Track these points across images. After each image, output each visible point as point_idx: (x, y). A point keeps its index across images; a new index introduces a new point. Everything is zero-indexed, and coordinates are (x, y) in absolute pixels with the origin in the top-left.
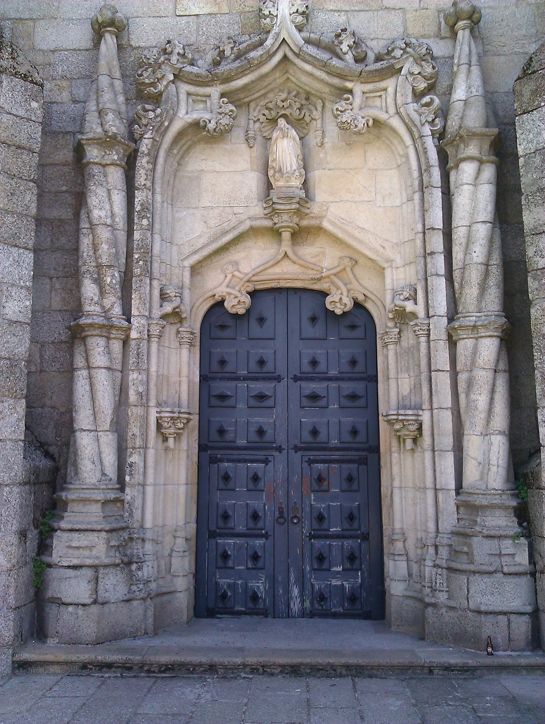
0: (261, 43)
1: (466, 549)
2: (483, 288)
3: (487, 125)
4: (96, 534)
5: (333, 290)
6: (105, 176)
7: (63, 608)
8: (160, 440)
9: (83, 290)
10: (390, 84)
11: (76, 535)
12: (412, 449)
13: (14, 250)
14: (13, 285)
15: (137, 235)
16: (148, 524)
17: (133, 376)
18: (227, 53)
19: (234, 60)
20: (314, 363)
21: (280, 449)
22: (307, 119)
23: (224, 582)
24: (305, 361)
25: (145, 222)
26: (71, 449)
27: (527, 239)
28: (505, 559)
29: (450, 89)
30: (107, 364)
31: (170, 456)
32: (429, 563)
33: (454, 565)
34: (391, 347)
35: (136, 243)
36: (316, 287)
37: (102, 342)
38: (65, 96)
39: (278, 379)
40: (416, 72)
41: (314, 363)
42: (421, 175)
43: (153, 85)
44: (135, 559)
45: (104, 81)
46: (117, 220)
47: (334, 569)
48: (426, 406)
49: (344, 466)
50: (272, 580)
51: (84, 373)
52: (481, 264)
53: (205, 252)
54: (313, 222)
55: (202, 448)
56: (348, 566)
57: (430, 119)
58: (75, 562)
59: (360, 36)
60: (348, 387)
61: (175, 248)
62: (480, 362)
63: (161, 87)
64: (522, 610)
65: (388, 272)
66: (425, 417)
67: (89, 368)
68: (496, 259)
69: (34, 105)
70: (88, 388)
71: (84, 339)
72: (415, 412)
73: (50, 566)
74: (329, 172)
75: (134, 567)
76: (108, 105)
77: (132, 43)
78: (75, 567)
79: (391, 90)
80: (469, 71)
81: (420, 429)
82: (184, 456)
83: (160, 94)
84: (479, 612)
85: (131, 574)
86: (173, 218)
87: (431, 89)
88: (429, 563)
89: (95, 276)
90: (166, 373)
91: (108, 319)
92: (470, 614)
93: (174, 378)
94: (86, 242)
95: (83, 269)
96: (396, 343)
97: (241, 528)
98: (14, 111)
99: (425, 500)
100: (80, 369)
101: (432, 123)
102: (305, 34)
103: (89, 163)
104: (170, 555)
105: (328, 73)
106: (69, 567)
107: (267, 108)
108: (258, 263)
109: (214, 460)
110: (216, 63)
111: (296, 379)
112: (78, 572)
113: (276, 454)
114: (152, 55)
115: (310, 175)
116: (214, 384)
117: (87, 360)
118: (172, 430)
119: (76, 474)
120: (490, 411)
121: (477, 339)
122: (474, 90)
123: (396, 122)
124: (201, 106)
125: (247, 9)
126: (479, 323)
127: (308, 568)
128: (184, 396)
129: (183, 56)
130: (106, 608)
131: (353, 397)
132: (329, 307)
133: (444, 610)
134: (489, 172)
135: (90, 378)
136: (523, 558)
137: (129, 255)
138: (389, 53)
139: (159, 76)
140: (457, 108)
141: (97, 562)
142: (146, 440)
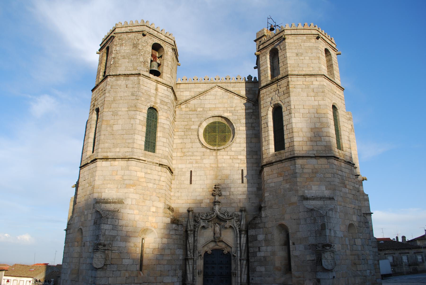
0: (214, 213)
2: (244, 253)
3: (245, 229)
10: (232, 220)
12: (235, 277)
15: (195, 244)
17: (195, 265)
20: (221, 262)
21: (216, 276)
34: (233, 260)
37: (190, 261)
38: (184, 220)
41: (221, 262)
43: (197, 220)
45: (190, 220)
51: (188, 265)
54: (221, 240)
55: (204, 275)
62: (243, 264)
63: (198, 221)
65: (232, 248)
66: (237, 272)
67: (189, 264)
71: (188, 260)
80: (244, 219)
87: (239, 220)
94: (188, 245)
102: (220, 212)
108: (213, 245)
110: (207, 216)
111: (219, 264)
114: (197, 215)
117: (188, 263)
119: (187, 279)
120: (245, 271)
123: (233, 226)
128: (201, 268)
129: (202, 216)
134: (246, 236)
137: (194, 247)
140: (242, 225)
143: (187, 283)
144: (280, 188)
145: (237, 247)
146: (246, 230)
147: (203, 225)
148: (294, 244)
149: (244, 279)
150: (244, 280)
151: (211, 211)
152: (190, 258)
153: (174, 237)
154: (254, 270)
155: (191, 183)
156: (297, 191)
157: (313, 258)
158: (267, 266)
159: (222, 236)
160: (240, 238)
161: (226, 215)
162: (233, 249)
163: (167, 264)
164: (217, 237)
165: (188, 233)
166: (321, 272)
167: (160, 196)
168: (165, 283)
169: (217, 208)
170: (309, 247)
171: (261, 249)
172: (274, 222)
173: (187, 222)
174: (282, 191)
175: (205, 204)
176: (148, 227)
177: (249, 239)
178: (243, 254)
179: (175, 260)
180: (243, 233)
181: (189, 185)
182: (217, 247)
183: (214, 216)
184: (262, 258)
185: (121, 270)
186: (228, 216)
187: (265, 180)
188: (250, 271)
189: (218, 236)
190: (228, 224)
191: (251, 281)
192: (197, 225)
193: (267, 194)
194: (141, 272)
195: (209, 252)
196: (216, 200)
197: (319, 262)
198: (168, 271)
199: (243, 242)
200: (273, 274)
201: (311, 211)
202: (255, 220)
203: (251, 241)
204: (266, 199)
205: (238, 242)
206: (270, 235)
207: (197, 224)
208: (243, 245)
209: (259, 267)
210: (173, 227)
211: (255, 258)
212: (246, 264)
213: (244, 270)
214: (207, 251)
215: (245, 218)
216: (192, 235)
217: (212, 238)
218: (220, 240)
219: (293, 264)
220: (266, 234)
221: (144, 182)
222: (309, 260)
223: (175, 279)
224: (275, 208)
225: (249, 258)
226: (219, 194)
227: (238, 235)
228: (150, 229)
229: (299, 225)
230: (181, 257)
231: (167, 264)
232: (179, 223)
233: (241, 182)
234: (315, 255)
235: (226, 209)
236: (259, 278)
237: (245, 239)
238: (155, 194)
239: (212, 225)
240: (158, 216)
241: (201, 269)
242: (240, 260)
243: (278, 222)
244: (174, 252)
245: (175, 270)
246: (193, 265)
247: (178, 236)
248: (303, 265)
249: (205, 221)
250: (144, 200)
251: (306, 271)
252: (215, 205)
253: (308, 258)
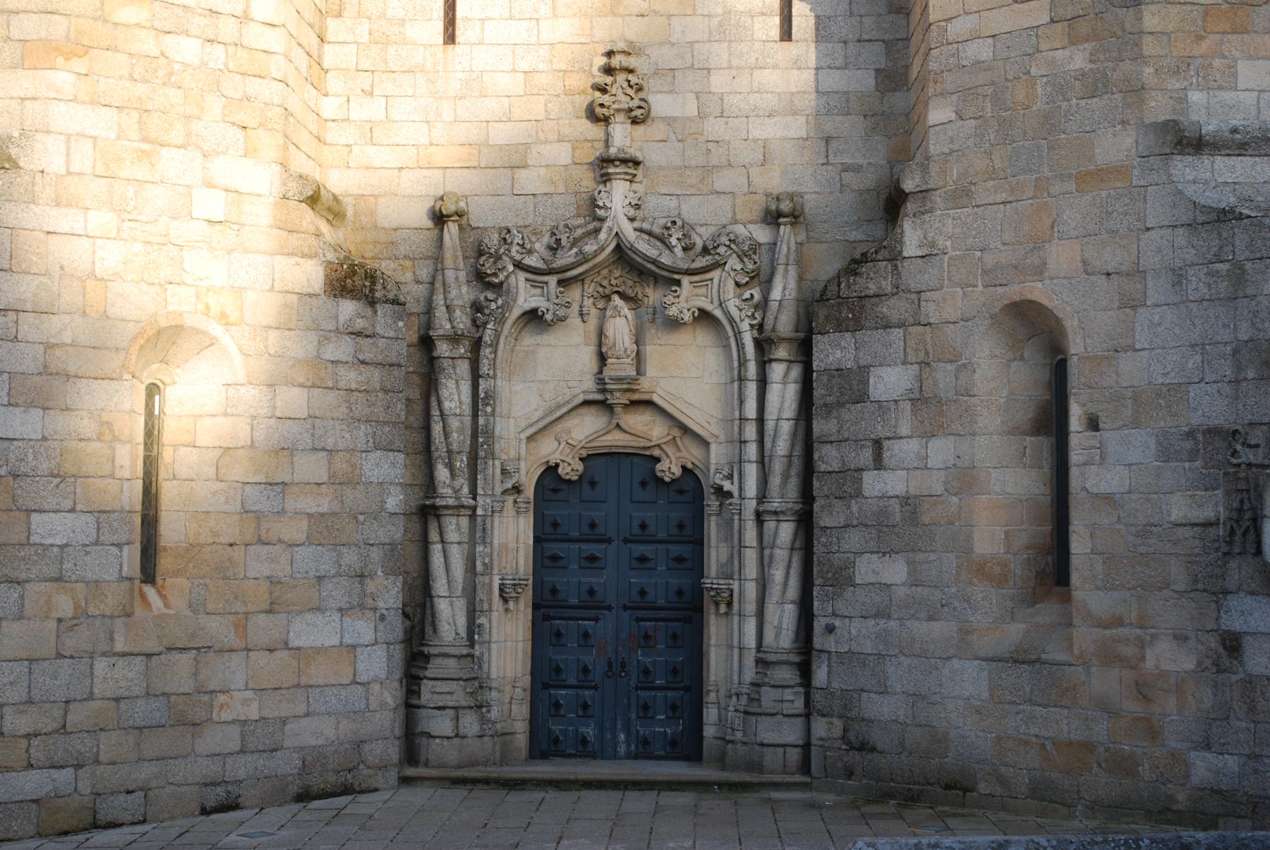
0: (597, 231)
1: (757, 697)
2: (786, 477)
3: (797, 331)
4: (455, 683)
5: (664, 457)
6: (454, 367)
7: (431, 740)
8: (501, 602)
9: (436, 473)
10: (715, 274)
11: (439, 683)
12: (726, 614)
13: (390, 454)
14: (391, 484)
15: (481, 421)
16: (494, 676)
17: (479, 548)
18: (564, 242)
19: (571, 249)
20: (643, 526)
21: (609, 608)
22: (640, 296)
23: (557, 729)
24: (636, 523)
25: (489, 409)
26: (428, 612)
27: (815, 444)
28: (786, 705)
29: (767, 284)
30: (458, 540)
31: (509, 616)
32: (731, 708)
33: (751, 709)
34: (713, 518)
35: (480, 428)
36: (647, 453)
37: (454, 520)
38: (408, 276)
39: (609, 541)
40: (739, 268)
41: (643, 526)
42: (740, 365)
43: (495, 275)
44: (484, 704)
45: (450, 274)
46: (464, 407)
47: (659, 717)
48: (736, 576)
49: (670, 624)
50: (601, 728)
51: (439, 546)
52: (784, 456)
53: (540, 425)
55: (536, 607)
56: (671, 715)
57: (750, 314)
58: (440, 704)
59: (690, 222)
60: (676, 549)
61: (512, 421)
63: (502, 277)
64: (796, 743)
65: (713, 447)
67: (442, 542)
68: (798, 451)
69: (401, 324)
70: (442, 560)
71: (438, 517)
72: (727, 581)
73: (419, 707)
74: (659, 348)
75: (484, 710)
76: (455, 302)
77: (472, 223)
78: (439, 708)
79: (716, 281)
80: (786, 271)
81: (731, 595)
82: (521, 616)
83: (501, 283)
84: (762, 745)
85: (482, 717)
86: (510, 392)
87: (754, 276)
88: (731, 708)
89: (447, 461)
90: (504, 541)
91: (457, 498)
92: (757, 747)
93: (512, 545)
94: (437, 429)
95: (436, 455)
96: (718, 515)
97: (572, 681)
98: (387, 335)
99: (732, 656)
100: (435, 543)
101: (753, 317)
102: (637, 224)
103: (439, 358)
104: (510, 703)
105: (658, 267)
106: (435, 708)
107: (601, 286)
108: (591, 431)
109: (547, 618)
110: (555, 248)
111: (626, 541)
112: (443, 712)
113: (606, 612)
114: (492, 241)
115: (642, 347)
116: (546, 545)
117: (441, 534)
118: (514, 595)
119: (435, 630)
120: (785, 584)
121: (778, 521)
122: (787, 293)
123: (718, 313)
124: (538, 291)
125: (583, 190)
126: (778, 510)
127: (634, 716)
128: (521, 562)
129: (522, 246)
130: (465, 741)
131: (680, 559)
132: (659, 474)
133: (739, 745)
134: (796, 372)
135: (444, 551)
136: (799, 704)
137: (475, 435)
138: (715, 248)
139: (500, 267)
140: (774, 306)
141: (457, 704)
142: (490, 605)
143: (434, 651)
144: (1029, 72)
145: (743, 442)
146: (801, 335)
147: (532, 303)
148: (1093, 424)
149: (779, 628)
150: (777, 636)
151: (581, 221)
152: (451, 502)
153: (351, 377)
154: (843, 579)
155: (450, 38)
156: (1136, 91)
157: (1208, 513)
158: (920, 556)
159: (651, 370)
160: (763, 383)
161: (673, 241)
162: (718, 454)
163: (309, 541)
164: (619, 380)
165: (435, 354)
166: (1252, 593)
167: (250, 123)
168: (298, 649)
169: (618, 196)
170: (1188, 445)
171: (886, 454)
172: (980, 288)
173: (432, 284)
174: (1039, 90)
175: (543, 171)
176: (181, 315)
177: (818, 392)
178: (775, 481)
179: (361, 518)
180: (782, 352)
181: (441, 48)
182: (616, 440)
183: (602, 249)
184: (895, 506)
185: (23, 576)
186: (685, 249)
187: (932, 19)
188: (818, 581)
189: (623, 374)
190: (688, 298)
191: (818, 642)
192: (493, 306)
193: (938, 113)
194: (150, 591)
195: (571, 469)
196: (613, 151)
197: (1244, 534)
198: (320, 579)
199: (780, 410)
200: (956, 604)
201: (1219, 220)
202: (856, 274)
203: (825, 405)
204: (935, 146)
205: (751, 409)
206: (950, 367)
207: (495, 301)
208: (777, 425)
209: (875, 556)
210: (342, 319)
211: (849, 507)
212: (794, 541)
213: (778, 574)
214: (557, 465)
215: (799, 262)
216: (464, 367)
217: (590, 384)
218: (636, 397)
219: (1079, 545)
220: (924, 364)
221: (138, 25)
222: (1185, 525)
223: (363, 629)
224: (991, 200)
225: (816, 507)
226: (631, 110)
227: (752, 369)
228: (193, 328)
229: (1134, 308)
230: (395, 501)
231: (309, 541)
232: (378, 295)
233: (775, 32)
234: (1219, 492)
235: (673, 203)
236: (871, 622)
237: (792, 390)
238: (215, 106)
239: (588, 302)
240: (246, 251)
241: (522, 569)
242: (759, 518)
243: (1000, 290)
244: (353, 466)
245: (362, 576)
246: (472, 542)
247: (376, 375)
248: (1142, 549)
249: (545, 278)
250: (146, 147)
251: (1160, 589)
252: (605, 179)
253: (1179, 508)
